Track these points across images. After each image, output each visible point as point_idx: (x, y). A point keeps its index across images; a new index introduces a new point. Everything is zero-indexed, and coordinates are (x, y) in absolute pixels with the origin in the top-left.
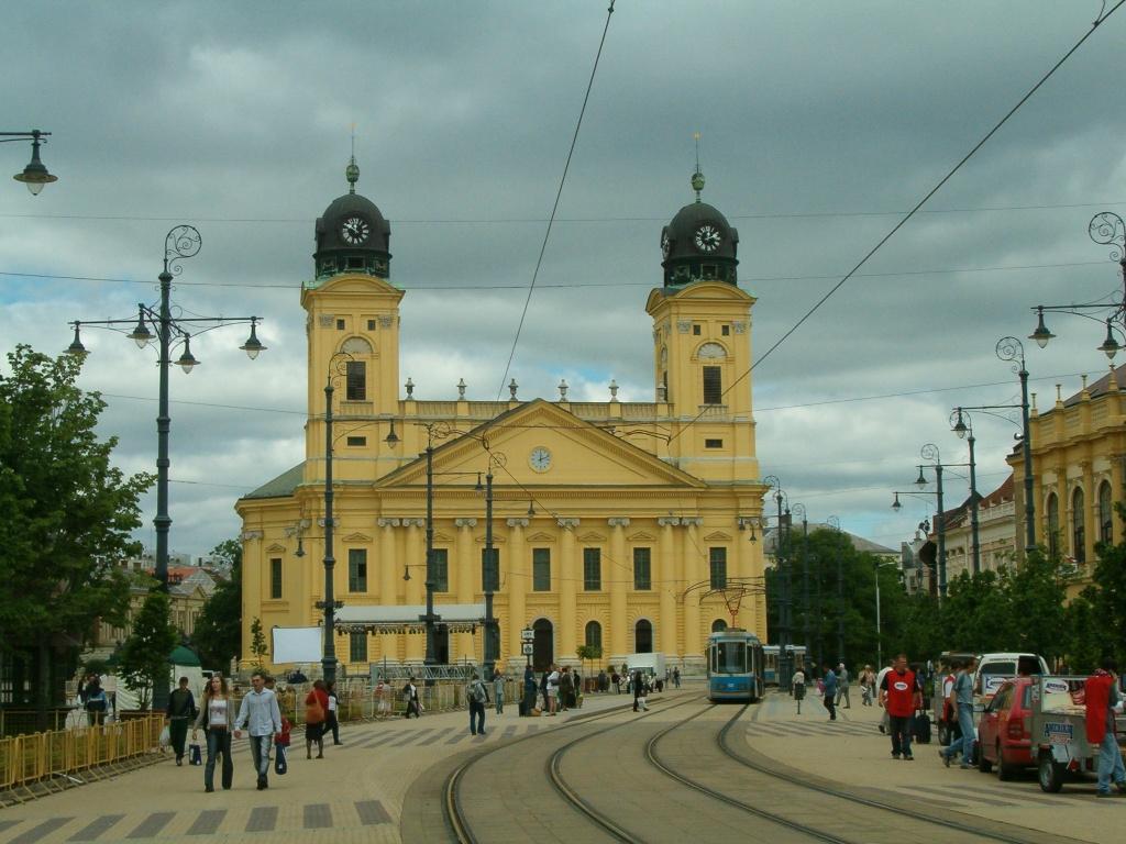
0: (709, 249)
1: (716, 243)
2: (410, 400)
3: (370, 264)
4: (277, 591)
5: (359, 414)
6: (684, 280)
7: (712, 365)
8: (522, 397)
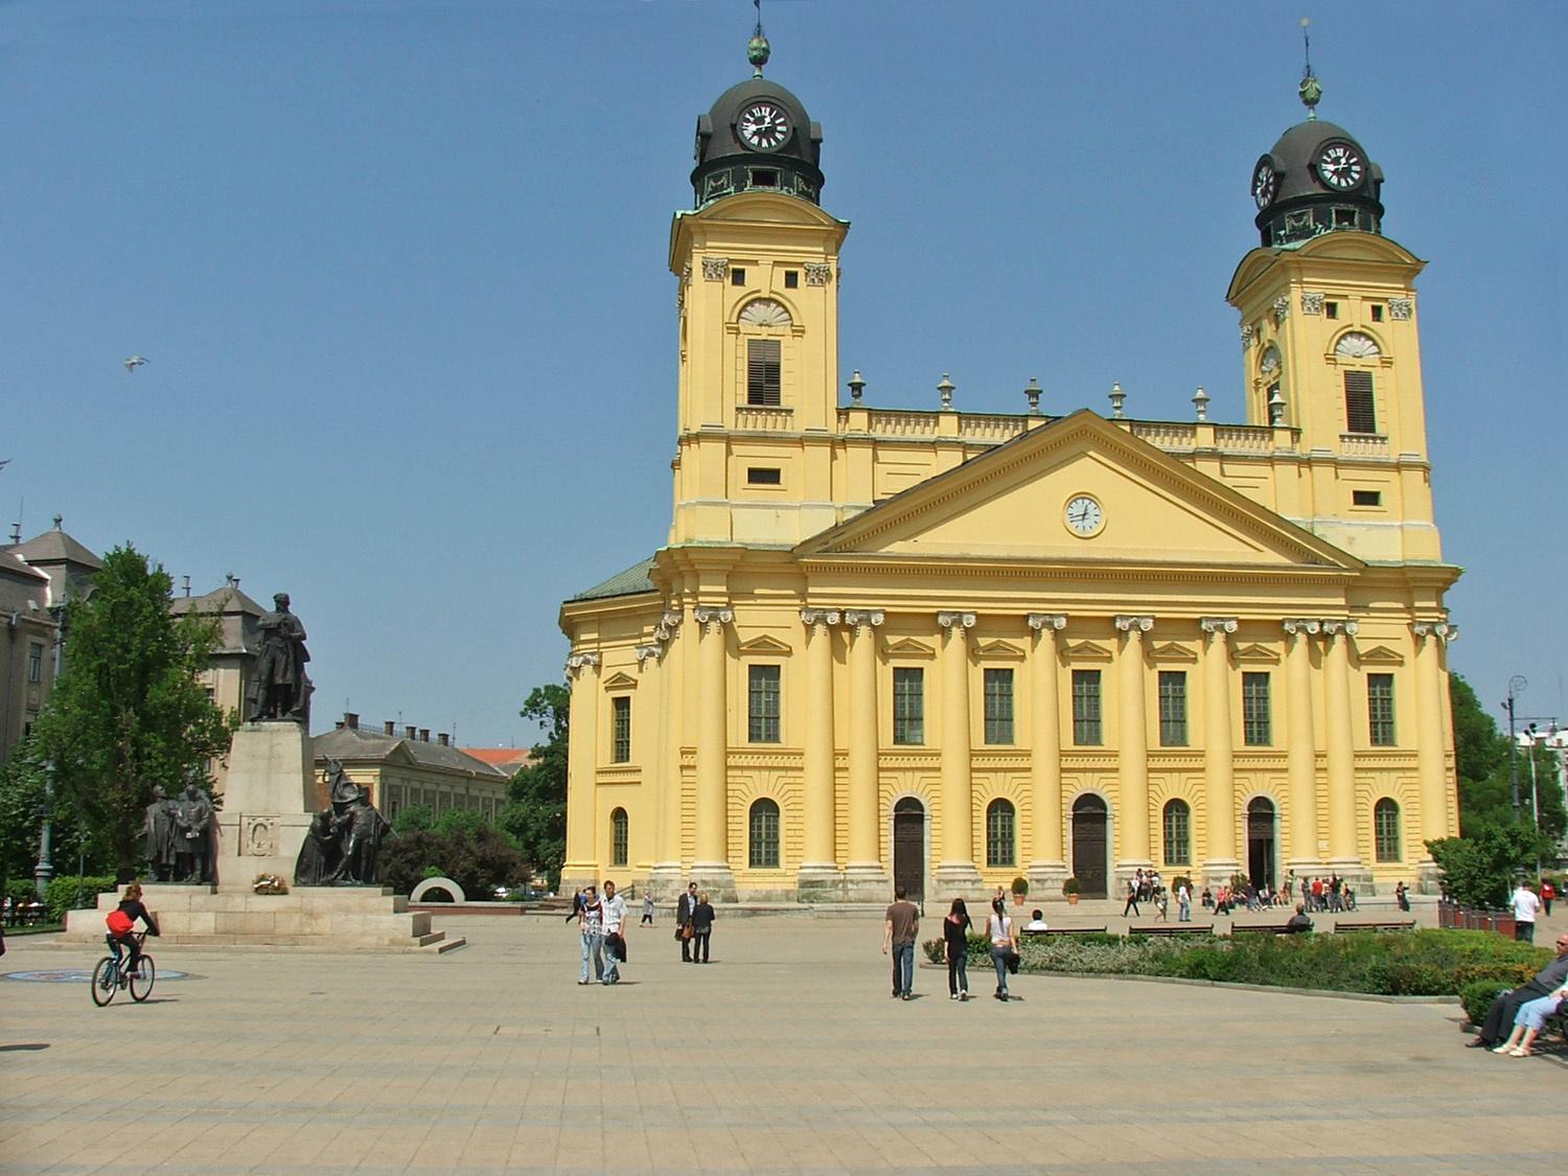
0: (1344, 184)
1: (1356, 176)
3: (788, 183)
4: (622, 750)
5: (769, 429)
6: (1305, 233)
7: (1358, 368)
8: (1048, 406)
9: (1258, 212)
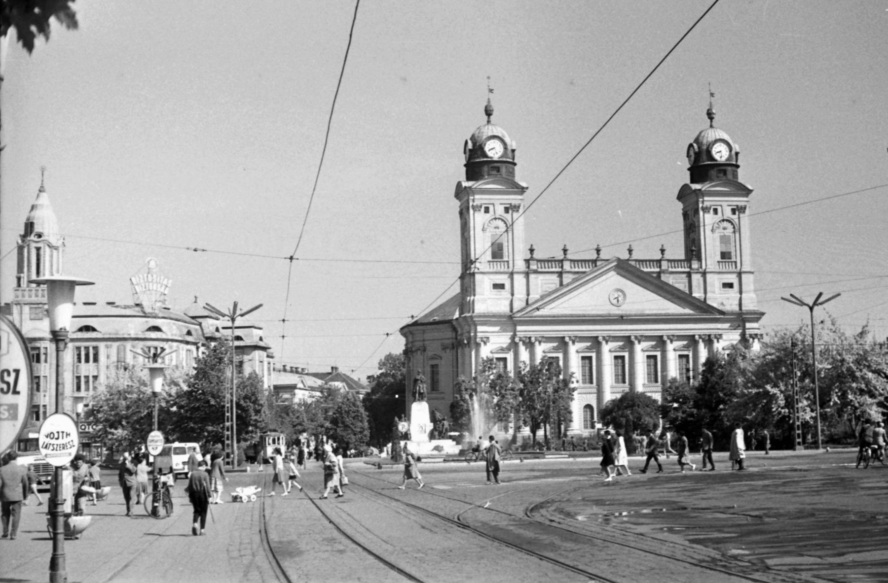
2: (532, 259)
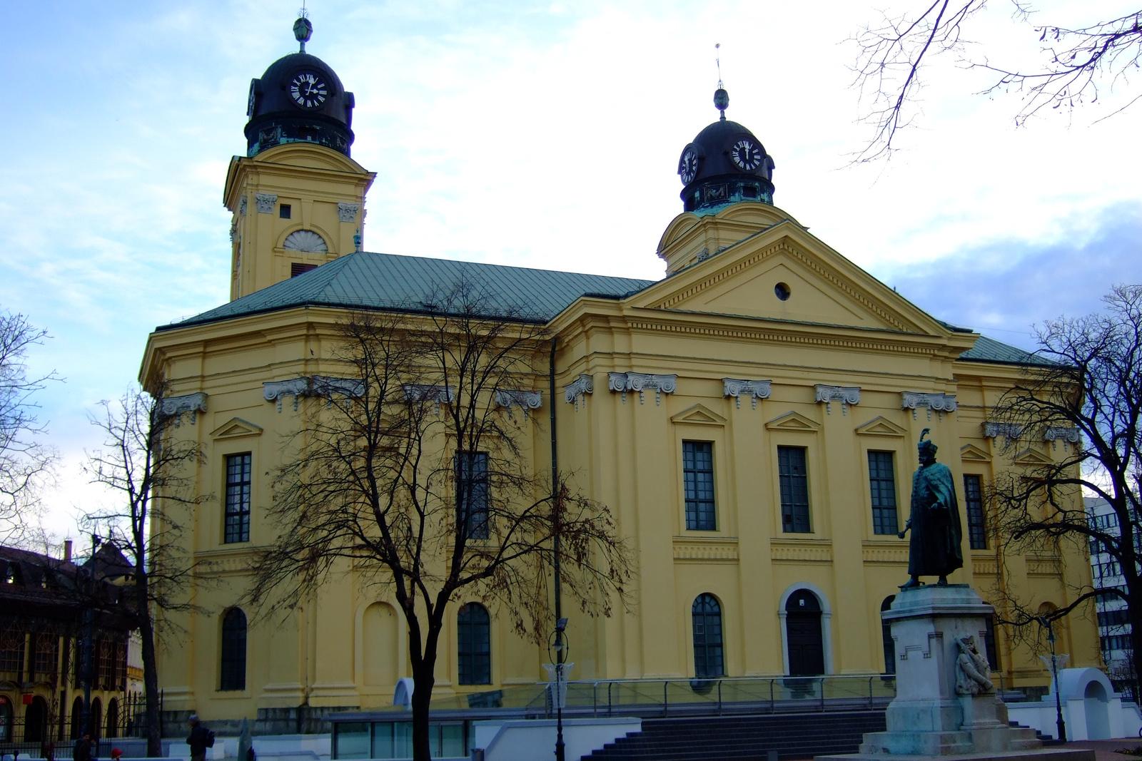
0: (748, 167)
1: (757, 163)
9: (684, 187)
